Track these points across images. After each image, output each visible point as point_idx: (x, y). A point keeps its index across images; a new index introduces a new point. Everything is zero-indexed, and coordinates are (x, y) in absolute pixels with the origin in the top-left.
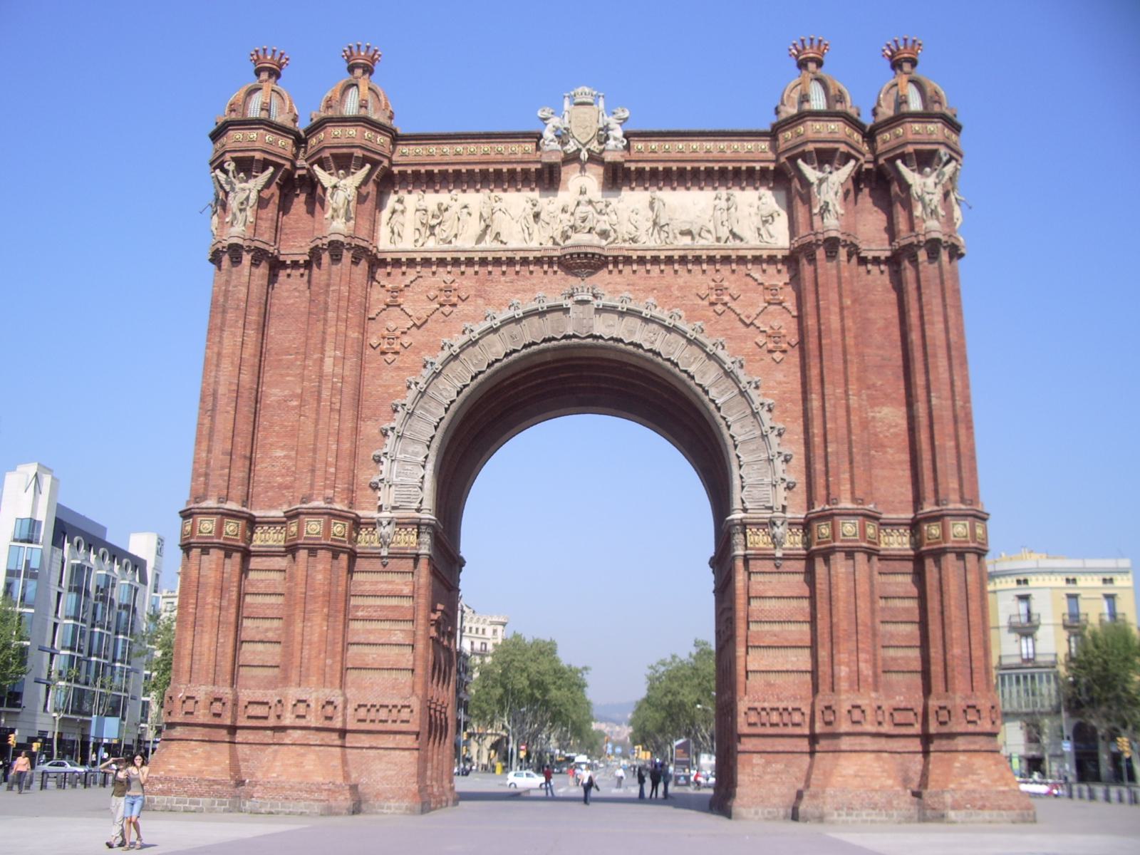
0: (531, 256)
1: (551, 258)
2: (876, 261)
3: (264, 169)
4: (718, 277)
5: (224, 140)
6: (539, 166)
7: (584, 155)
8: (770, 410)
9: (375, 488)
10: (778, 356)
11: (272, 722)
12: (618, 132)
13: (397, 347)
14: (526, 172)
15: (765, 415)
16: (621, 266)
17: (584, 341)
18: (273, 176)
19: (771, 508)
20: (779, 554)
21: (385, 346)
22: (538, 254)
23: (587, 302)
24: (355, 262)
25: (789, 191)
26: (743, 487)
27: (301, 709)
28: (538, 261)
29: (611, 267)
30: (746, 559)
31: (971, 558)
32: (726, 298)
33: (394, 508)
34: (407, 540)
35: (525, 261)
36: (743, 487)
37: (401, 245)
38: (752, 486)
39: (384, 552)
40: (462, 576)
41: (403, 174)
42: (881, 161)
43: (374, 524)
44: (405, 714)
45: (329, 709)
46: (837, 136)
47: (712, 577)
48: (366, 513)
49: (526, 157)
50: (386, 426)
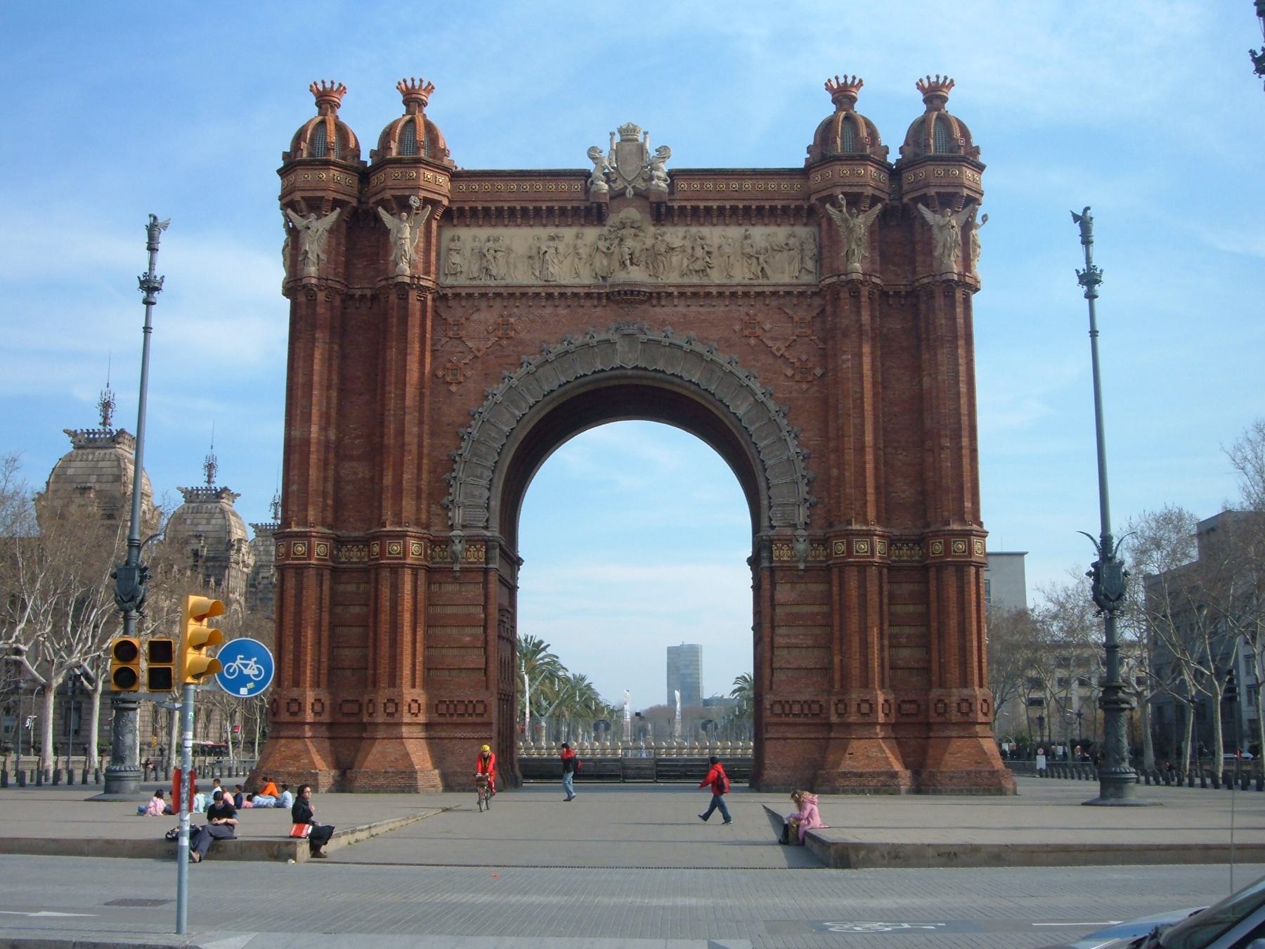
0: (582, 291)
2: (897, 294)
3: (333, 210)
5: (292, 178)
6: (588, 204)
7: (630, 192)
8: (796, 436)
9: (447, 508)
10: (804, 386)
11: (365, 720)
13: (461, 379)
14: (576, 210)
16: (663, 303)
17: (630, 373)
18: (340, 215)
19: (794, 526)
20: (802, 566)
21: (448, 379)
22: (586, 290)
25: (819, 225)
26: (770, 507)
28: (588, 296)
29: (654, 302)
30: (772, 570)
32: (759, 332)
33: (464, 526)
34: (475, 556)
35: (575, 295)
37: (462, 280)
38: (779, 505)
39: (457, 567)
40: (520, 574)
41: (461, 210)
42: (905, 200)
43: (448, 541)
44: (480, 709)
46: (861, 181)
47: (750, 574)
48: (436, 530)
50: (454, 452)
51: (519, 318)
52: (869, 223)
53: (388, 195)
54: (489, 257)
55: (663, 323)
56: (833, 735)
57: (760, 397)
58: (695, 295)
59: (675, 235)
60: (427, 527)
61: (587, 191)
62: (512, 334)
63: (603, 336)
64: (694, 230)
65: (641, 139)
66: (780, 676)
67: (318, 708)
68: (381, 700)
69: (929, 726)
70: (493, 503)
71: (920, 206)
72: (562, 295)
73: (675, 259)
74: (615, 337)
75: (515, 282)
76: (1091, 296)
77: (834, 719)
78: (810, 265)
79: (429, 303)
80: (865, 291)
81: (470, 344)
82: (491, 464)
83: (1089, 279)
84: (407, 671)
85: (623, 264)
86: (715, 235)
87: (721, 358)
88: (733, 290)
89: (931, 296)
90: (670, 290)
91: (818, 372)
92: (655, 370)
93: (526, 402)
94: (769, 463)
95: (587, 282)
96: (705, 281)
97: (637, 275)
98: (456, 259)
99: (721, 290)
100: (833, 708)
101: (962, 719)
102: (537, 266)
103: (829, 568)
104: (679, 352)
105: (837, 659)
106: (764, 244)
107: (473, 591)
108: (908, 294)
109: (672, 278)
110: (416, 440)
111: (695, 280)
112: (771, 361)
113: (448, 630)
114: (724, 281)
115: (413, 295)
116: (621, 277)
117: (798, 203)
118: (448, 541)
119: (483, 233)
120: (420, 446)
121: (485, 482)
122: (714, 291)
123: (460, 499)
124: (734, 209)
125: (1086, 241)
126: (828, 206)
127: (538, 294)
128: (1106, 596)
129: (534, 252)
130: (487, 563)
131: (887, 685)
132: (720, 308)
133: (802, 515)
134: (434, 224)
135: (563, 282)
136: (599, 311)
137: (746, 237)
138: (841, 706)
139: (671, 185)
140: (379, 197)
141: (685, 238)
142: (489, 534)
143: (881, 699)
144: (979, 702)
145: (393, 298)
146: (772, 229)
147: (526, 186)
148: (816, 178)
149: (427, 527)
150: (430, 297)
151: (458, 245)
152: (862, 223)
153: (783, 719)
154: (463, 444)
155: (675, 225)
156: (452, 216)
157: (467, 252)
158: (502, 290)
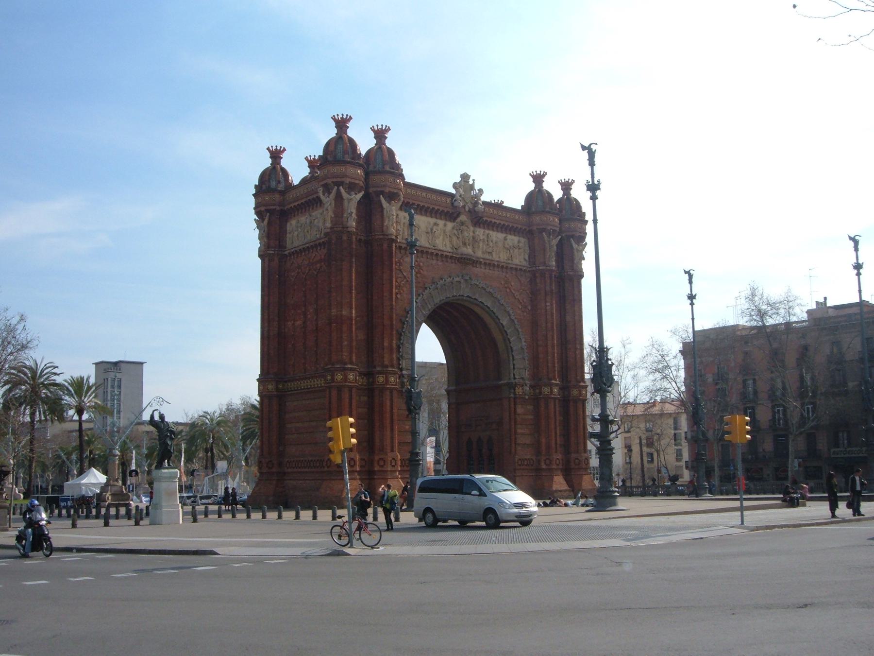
3: (360, 192)
15: (523, 340)
19: (523, 378)
28: (451, 257)
36: (514, 368)
53: (387, 190)
57: (513, 318)
58: (490, 264)
59: (480, 232)
61: (452, 204)
63: (457, 279)
64: (487, 232)
65: (471, 182)
66: (519, 448)
76: (692, 304)
77: (544, 467)
78: (527, 257)
83: (691, 297)
85: (465, 244)
91: (529, 308)
94: (514, 348)
95: (450, 250)
96: (490, 258)
97: (468, 250)
104: (483, 291)
105: (543, 440)
106: (511, 244)
111: (487, 256)
114: (497, 259)
127: (432, 253)
132: (497, 273)
133: (526, 374)
137: (505, 239)
138: (548, 462)
145: (385, 246)
146: (513, 237)
147: (429, 196)
148: (537, 219)
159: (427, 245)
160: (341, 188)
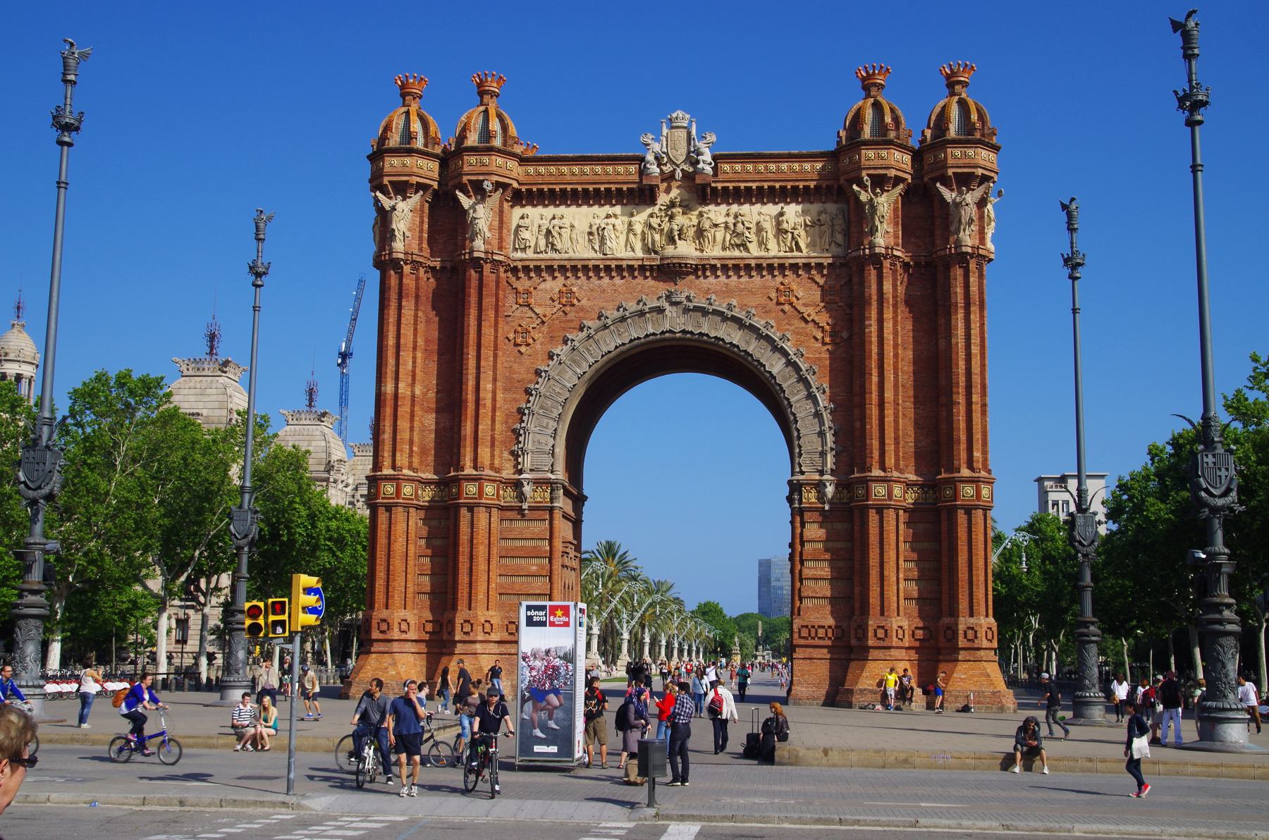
1: (651, 266)
4: (786, 281)
7: (679, 174)
12: (707, 156)
13: (531, 341)
21: (519, 341)
22: (640, 263)
23: (680, 303)
24: (494, 270)
27: (467, 628)
28: (642, 268)
31: (979, 513)
32: (794, 299)
35: (631, 268)
37: (530, 254)
42: (926, 179)
45: (487, 625)
48: (508, 473)
49: (630, 178)
51: (581, 287)
52: (893, 199)
54: (555, 233)
55: (708, 291)
56: (852, 656)
58: (736, 268)
59: (717, 213)
60: (498, 470)
61: (642, 172)
62: (575, 301)
67: (404, 626)
68: (459, 621)
69: (938, 651)
70: (557, 450)
71: (938, 185)
72: (619, 268)
73: (720, 234)
74: (667, 305)
75: (577, 255)
77: (854, 642)
78: (839, 238)
79: (502, 275)
80: (887, 263)
81: (537, 311)
82: (555, 414)
84: (481, 596)
86: (754, 213)
87: (759, 322)
88: (769, 262)
89: (948, 268)
90: (713, 262)
91: (845, 335)
92: (700, 334)
93: (586, 361)
95: (640, 254)
96: (744, 254)
98: (525, 234)
99: (759, 262)
100: (852, 633)
101: (969, 645)
102: (596, 239)
103: (851, 510)
105: (857, 590)
107: (541, 528)
108: (928, 264)
109: (714, 252)
110: (490, 396)
111: (736, 253)
112: (803, 324)
113: (518, 561)
114: (763, 254)
115: (487, 268)
116: (670, 251)
117: (829, 183)
118: (518, 485)
119: (551, 211)
120: (494, 400)
121: (550, 431)
122: (753, 263)
123: (530, 446)
124: (772, 188)
125: (1071, 230)
126: (855, 187)
128: (1080, 542)
129: (595, 228)
130: (552, 500)
131: (901, 613)
134: (506, 205)
135: (619, 256)
136: (650, 282)
137: (781, 214)
138: (860, 631)
139: (715, 169)
140: (456, 181)
141: (728, 215)
142: (553, 477)
143: (895, 627)
144: (984, 629)
146: (808, 206)
147: (587, 169)
149: (498, 470)
150: (502, 270)
151: (526, 222)
152: (886, 203)
153: (810, 642)
154: (532, 399)
155: (718, 204)
156: (520, 197)
157: (535, 229)
158: (566, 263)
159: (592, 255)
160: (378, 194)
